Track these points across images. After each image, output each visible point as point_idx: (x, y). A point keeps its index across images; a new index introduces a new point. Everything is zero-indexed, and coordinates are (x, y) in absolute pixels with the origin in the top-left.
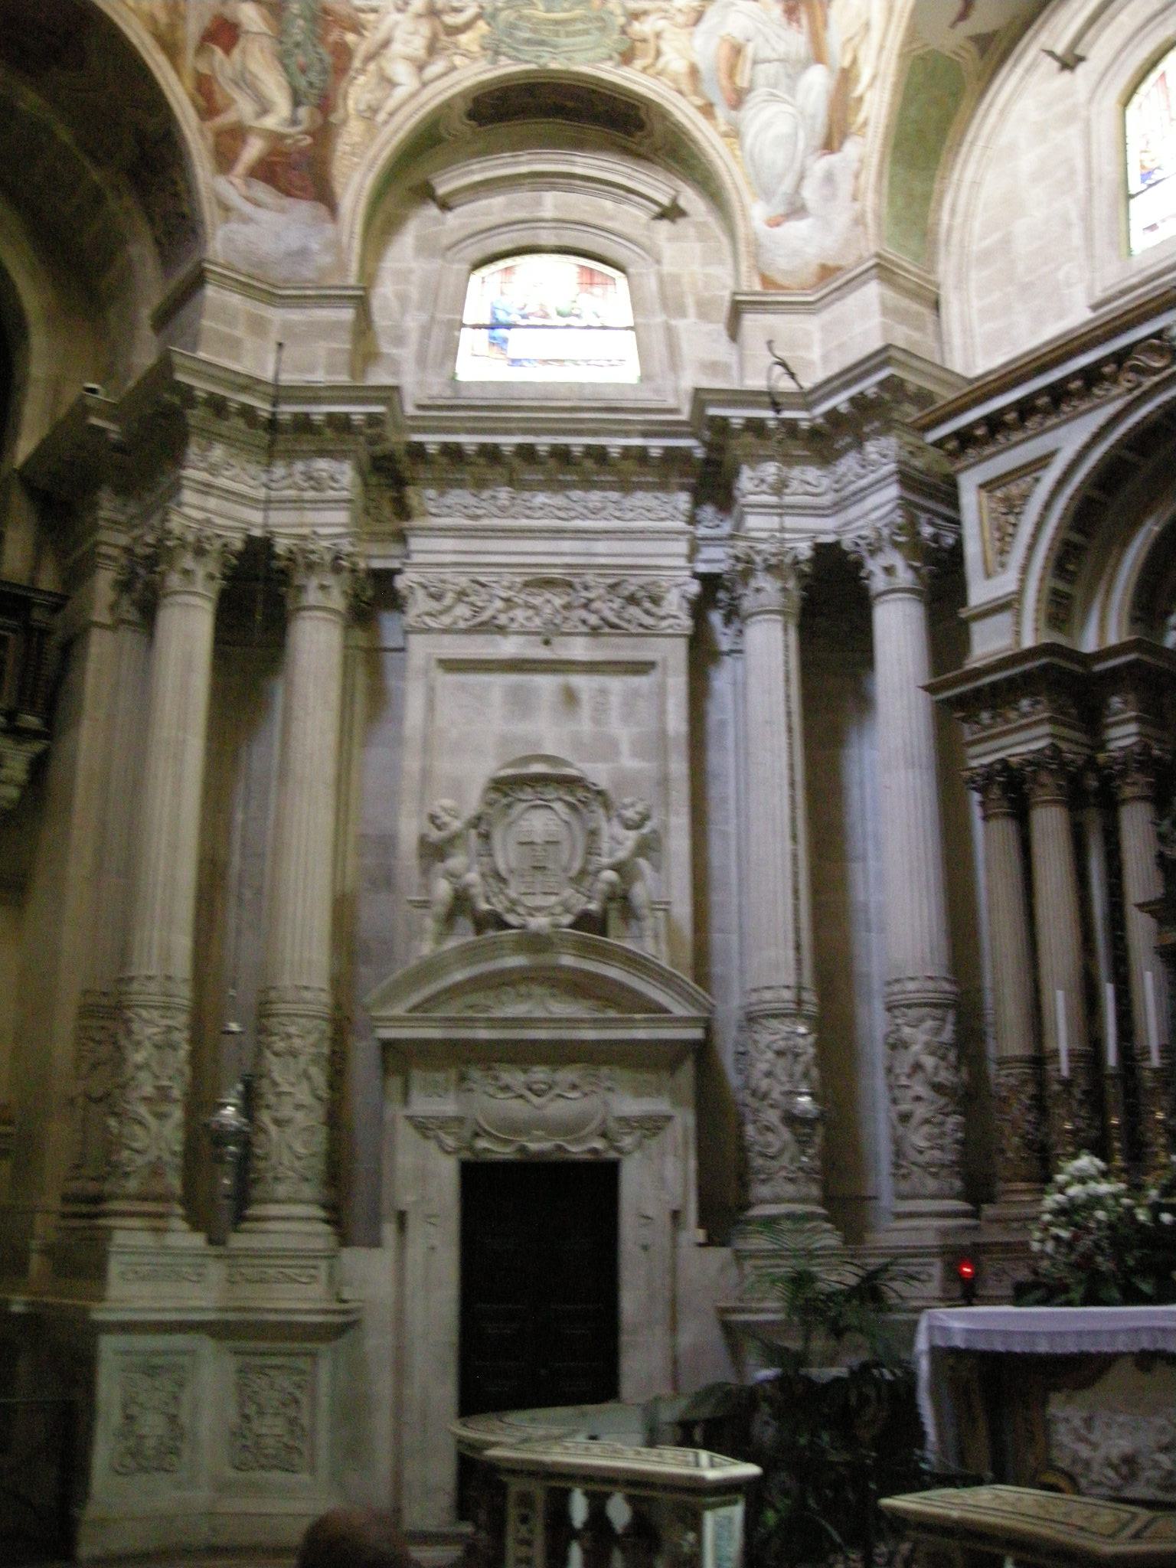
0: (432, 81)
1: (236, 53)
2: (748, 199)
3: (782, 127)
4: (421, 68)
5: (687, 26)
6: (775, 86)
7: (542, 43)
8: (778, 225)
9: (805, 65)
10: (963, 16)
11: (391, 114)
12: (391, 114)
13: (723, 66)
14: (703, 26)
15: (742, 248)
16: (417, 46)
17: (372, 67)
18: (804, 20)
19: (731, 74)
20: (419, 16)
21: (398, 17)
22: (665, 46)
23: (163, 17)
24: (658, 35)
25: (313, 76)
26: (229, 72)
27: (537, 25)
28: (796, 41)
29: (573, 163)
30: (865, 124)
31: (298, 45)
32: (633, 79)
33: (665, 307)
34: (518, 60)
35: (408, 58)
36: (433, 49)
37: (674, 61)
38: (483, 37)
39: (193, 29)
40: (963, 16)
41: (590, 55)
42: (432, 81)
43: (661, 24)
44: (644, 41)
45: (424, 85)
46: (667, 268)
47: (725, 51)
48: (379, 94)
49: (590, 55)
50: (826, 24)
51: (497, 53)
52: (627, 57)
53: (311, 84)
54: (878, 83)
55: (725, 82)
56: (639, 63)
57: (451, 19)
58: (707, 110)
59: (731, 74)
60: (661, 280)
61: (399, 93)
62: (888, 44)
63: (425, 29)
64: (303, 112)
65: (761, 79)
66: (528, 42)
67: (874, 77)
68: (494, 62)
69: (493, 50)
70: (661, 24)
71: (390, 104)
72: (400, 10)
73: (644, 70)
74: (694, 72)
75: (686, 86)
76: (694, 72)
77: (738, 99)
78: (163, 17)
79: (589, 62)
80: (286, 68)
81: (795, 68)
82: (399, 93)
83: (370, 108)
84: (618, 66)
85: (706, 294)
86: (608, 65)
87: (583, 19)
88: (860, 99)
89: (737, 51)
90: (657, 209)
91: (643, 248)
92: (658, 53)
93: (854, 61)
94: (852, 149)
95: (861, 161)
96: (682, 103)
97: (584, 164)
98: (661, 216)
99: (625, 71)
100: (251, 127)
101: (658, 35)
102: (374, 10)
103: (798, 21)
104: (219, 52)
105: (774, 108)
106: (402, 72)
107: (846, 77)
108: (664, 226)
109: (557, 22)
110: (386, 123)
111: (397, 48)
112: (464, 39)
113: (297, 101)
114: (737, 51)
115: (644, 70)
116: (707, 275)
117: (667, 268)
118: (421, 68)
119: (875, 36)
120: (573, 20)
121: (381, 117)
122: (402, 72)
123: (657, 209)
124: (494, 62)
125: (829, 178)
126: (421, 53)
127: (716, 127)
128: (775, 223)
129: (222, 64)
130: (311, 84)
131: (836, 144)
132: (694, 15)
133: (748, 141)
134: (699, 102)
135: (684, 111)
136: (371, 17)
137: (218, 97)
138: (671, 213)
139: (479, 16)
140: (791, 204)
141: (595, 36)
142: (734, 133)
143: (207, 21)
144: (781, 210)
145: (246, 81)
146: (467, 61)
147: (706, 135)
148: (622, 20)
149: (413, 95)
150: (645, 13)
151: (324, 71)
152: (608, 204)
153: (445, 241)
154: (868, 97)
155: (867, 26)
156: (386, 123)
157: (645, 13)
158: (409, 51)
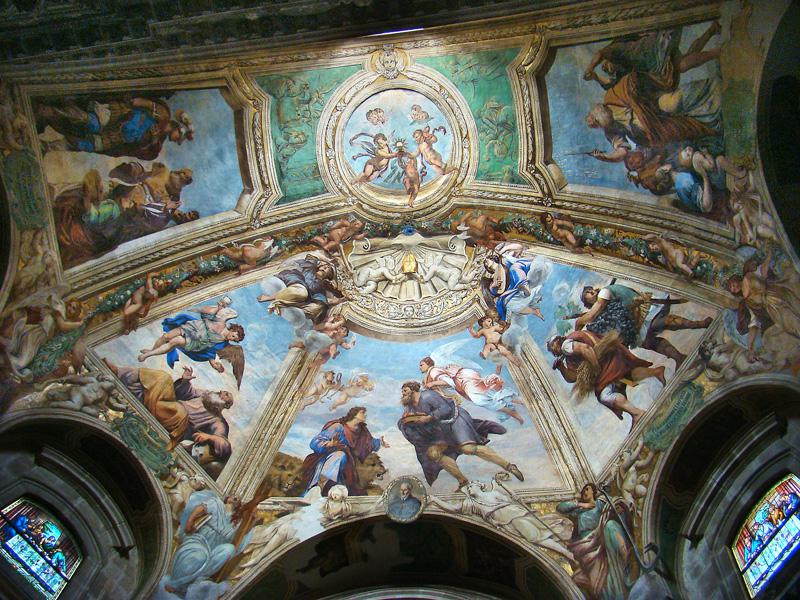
0: (84, 412)
1: (30, 326)
2: (165, 570)
3: (199, 556)
4: (85, 404)
5: (193, 487)
6: (208, 539)
7: (137, 442)
8: (170, 592)
9: (226, 541)
10: (304, 570)
11: (59, 407)
12: (59, 407)
13: (194, 514)
14: (199, 493)
15: (148, 587)
16: (93, 396)
17: (69, 385)
18: (238, 525)
19: (196, 519)
20: (103, 388)
21: (95, 380)
22: (179, 486)
23: (22, 285)
24: (181, 481)
25: (44, 364)
26: (21, 328)
27: (141, 433)
28: (230, 530)
29: (103, 497)
30: (239, 579)
31: (51, 350)
32: (159, 486)
33: (92, 585)
34: (123, 438)
35: (84, 396)
36: (96, 403)
37: (179, 494)
38: (118, 418)
39: (28, 301)
40: (304, 570)
41: (150, 462)
42: (84, 412)
43: (185, 478)
44: (174, 478)
45: (81, 411)
46: (104, 570)
47: (199, 509)
48: (61, 396)
49: (150, 462)
50: (247, 532)
51: (117, 428)
52: (163, 477)
53: (40, 366)
54: (255, 568)
55: (190, 520)
56: (165, 483)
57: (112, 401)
58: (176, 524)
59: (196, 519)
60: (98, 574)
61: (69, 404)
62: (270, 556)
63: (100, 395)
64: (27, 372)
65: (204, 532)
66: (132, 436)
67: (254, 565)
68: (114, 430)
69: (117, 425)
70: (185, 478)
71: (62, 404)
72: (97, 379)
73: (165, 487)
74: (182, 505)
75: (175, 507)
76: (182, 505)
77: (191, 531)
78: (22, 285)
79: (147, 464)
80: (39, 352)
81: (221, 539)
82: (69, 404)
83: (53, 396)
84: (157, 476)
85: (111, 597)
86: (154, 473)
87: (159, 449)
88: (243, 569)
89: (204, 513)
90: (120, 545)
91: (102, 554)
92: (175, 487)
93: (250, 553)
94: (224, 586)
95: (226, 593)
96: (169, 512)
97: (106, 500)
98: (117, 549)
99: (158, 481)
100: (5, 353)
101: (181, 481)
102: (90, 371)
103: (236, 523)
104: (25, 319)
105: (198, 546)
106: (77, 399)
107: (240, 557)
108: (115, 555)
109: (148, 440)
110: (53, 407)
111: (84, 389)
112: (111, 411)
113: (28, 366)
114: (204, 513)
115: (165, 487)
116: (117, 589)
117: (104, 570)
118: (85, 404)
119: (266, 550)
120: (156, 446)
121: (54, 404)
122: (77, 399)
123: (120, 545)
124: (114, 430)
125: (205, 590)
126: (91, 400)
127: (174, 533)
128: (168, 589)
129: (21, 323)
130: (40, 366)
131: (218, 579)
132: (198, 487)
133: (183, 549)
134: (175, 517)
135: (167, 516)
136: (86, 371)
137: (7, 331)
138: (123, 552)
139: (122, 410)
140: (181, 589)
141: (158, 458)
142: (179, 542)
143: (34, 305)
144: (175, 587)
145: (22, 339)
146: (104, 419)
147: (169, 533)
148: (173, 463)
149: (72, 409)
150: (183, 469)
151: (50, 368)
152: (102, 525)
153: (26, 474)
154: (246, 570)
155: (266, 544)
156: (53, 407)
157: (183, 469)
158: (87, 394)
